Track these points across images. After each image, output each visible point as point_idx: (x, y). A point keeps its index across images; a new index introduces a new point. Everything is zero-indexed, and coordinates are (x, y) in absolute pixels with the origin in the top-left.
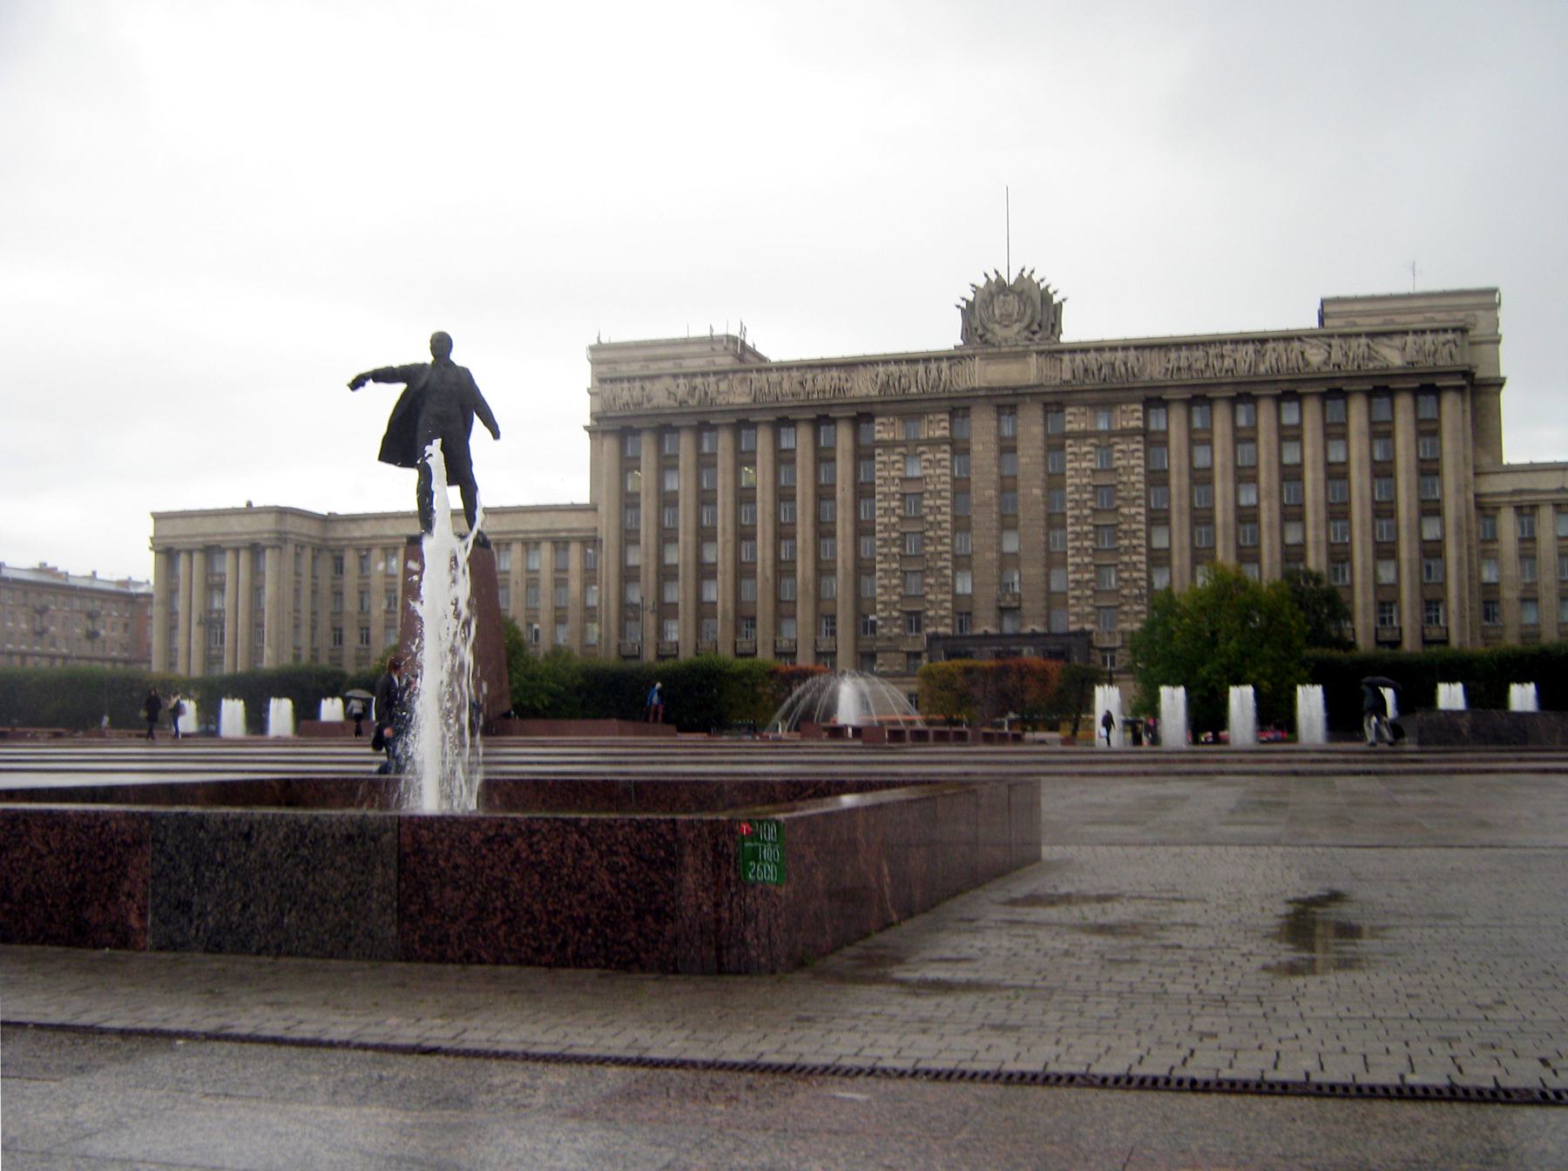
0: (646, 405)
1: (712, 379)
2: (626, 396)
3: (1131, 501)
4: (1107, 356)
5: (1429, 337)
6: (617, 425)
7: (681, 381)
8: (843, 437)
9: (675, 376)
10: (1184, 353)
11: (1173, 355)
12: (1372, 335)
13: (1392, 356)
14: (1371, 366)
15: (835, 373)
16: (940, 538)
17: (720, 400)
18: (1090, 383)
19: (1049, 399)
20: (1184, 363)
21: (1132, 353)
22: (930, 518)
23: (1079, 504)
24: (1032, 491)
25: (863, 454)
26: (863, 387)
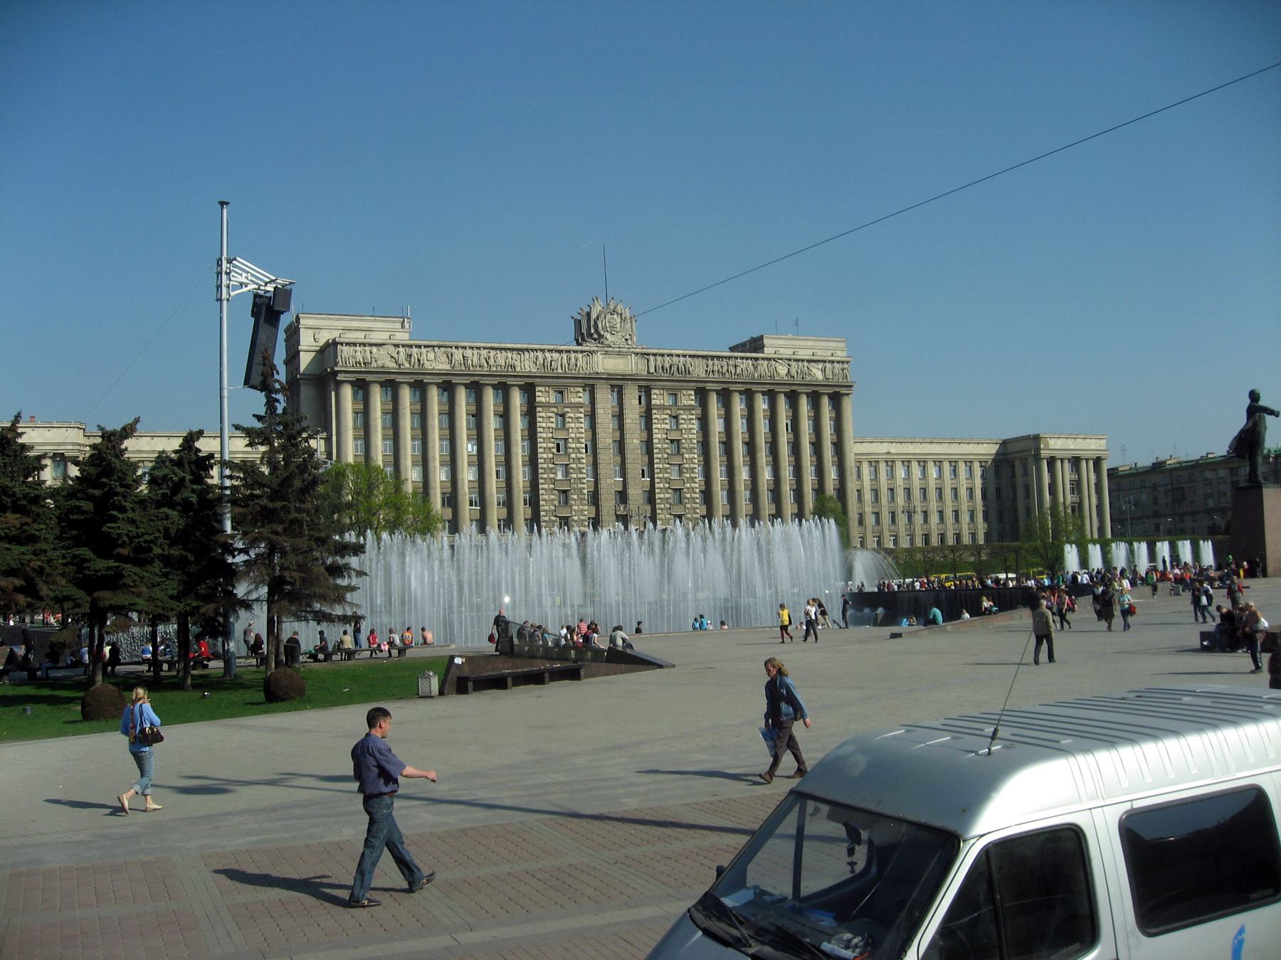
0: (374, 364)
1: (424, 350)
2: (359, 357)
3: (691, 450)
4: (675, 359)
5: (836, 365)
6: (352, 377)
7: (401, 349)
8: (517, 399)
9: (397, 346)
10: (716, 362)
11: (710, 363)
12: (809, 361)
13: (817, 373)
14: (808, 378)
15: (509, 354)
16: (580, 469)
17: (428, 366)
18: (666, 376)
19: (642, 383)
20: (716, 368)
21: (689, 359)
22: (573, 456)
23: (662, 450)
24: (634, 441)
25: (530, 413)
26: (526, 365)
